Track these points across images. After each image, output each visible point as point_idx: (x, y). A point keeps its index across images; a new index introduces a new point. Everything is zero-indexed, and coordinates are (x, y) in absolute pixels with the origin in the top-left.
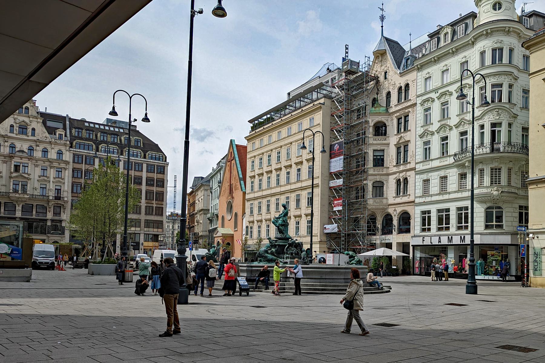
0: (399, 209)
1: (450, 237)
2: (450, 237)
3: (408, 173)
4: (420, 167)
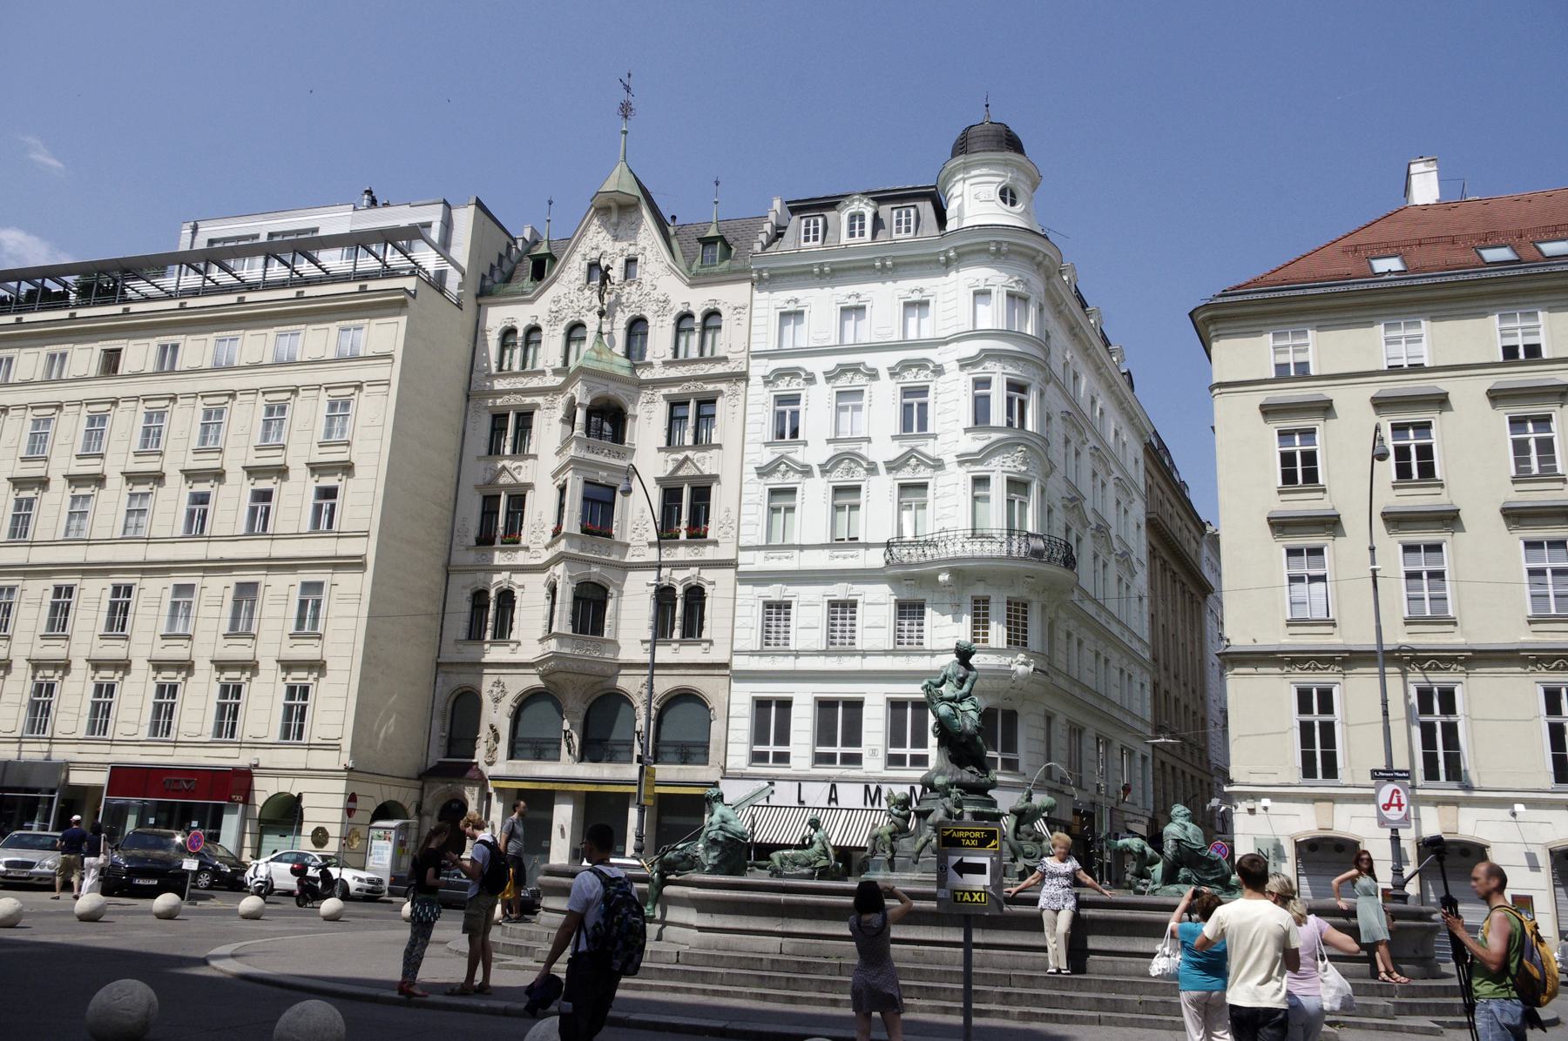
0: (665, 684)
1: (873, 788)
2: (873, 788)
3: (708, 575)
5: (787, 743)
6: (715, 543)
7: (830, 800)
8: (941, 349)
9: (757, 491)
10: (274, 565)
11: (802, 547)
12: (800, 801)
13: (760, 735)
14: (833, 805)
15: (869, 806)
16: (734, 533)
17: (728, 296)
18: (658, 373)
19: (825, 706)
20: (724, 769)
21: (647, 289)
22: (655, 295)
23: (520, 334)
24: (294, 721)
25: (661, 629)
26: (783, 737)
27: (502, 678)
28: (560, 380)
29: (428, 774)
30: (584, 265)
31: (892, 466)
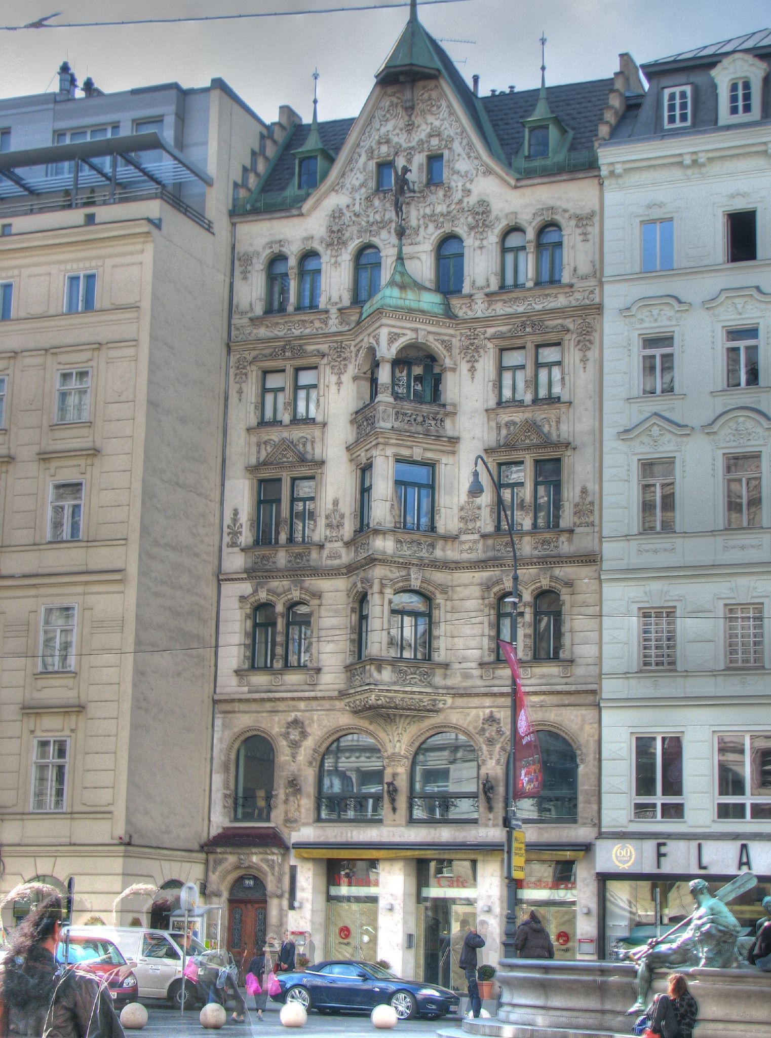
5: (678, 792)
7: (741, 864)
12: (701, 867)
13: (645, 784)
18: (480, 308)
21: (458, 195)
26: (673, 786)
30: (372, 165)
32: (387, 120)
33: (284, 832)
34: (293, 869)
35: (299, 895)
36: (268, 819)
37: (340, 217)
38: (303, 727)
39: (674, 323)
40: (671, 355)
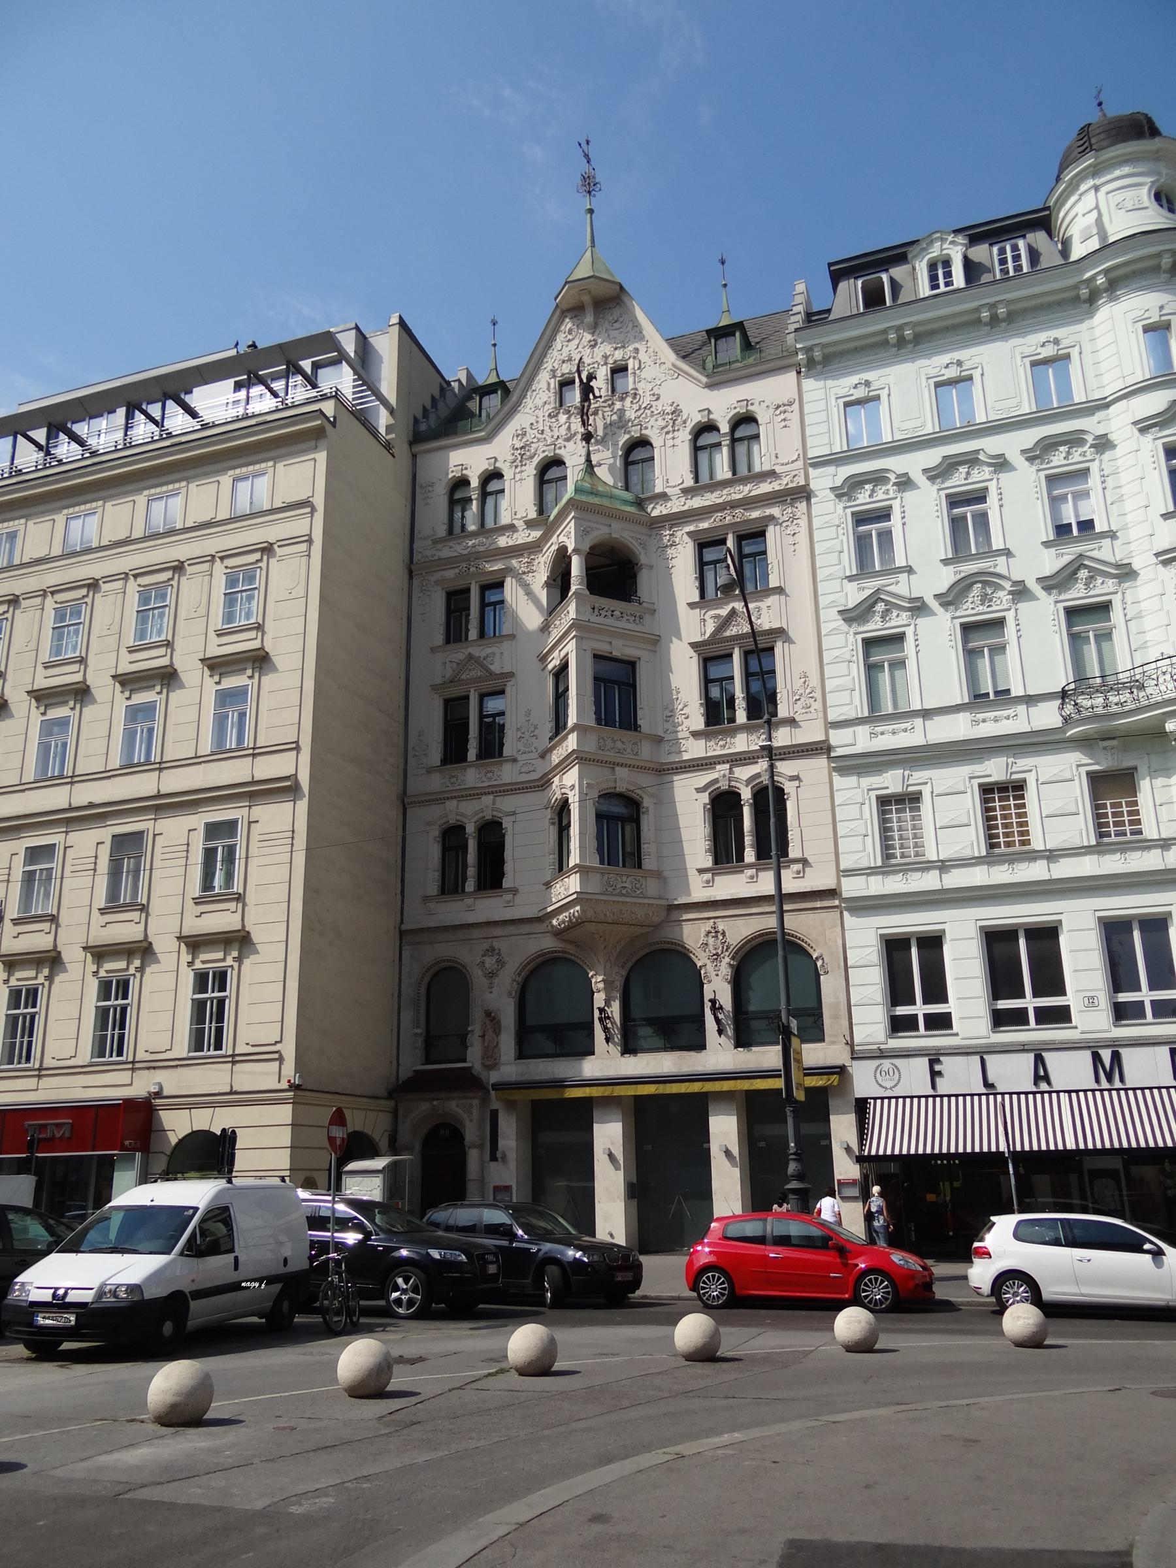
0: (741, 929)
1: (1106, 1055)
2: (1106, 1055)
4: (862, 740)
6: (792, 722)
7: (1037, 1079)
8: (1099, 415)
9: (844, 645)
10: (164, 805)
11: (926, 714)
12: (987, 1084)
13: (898, 991)
14: (1044, 1086)
15: (1105, 1084)
16: (818, 705)
17: (764, 393)
18: (676, 505)
19: (997, 942)
20: (851, 1044)
22: (658, 406)
23: (475, 483)
24: (209, 1024)
25: (725, 852)
26: (936, 990)
27: (496, 945)
28: (536, 534)
29: (404, 1089)
30: (554, 384)
31: (1055, 583)
32: (569, 341)
33: (483, 1075)
34: (494, 1115)
35: (502, 1143)
36: (464, 1061)
37: (524, 434)
38: (499, 954)
39: (892, 495)
40: (889, 533)
